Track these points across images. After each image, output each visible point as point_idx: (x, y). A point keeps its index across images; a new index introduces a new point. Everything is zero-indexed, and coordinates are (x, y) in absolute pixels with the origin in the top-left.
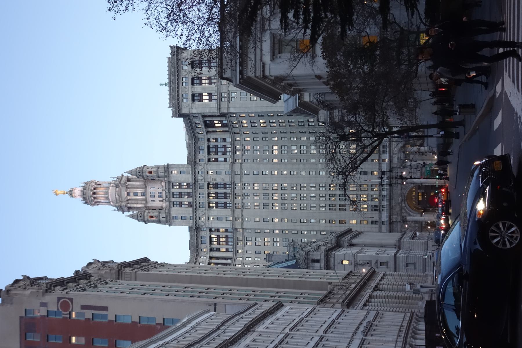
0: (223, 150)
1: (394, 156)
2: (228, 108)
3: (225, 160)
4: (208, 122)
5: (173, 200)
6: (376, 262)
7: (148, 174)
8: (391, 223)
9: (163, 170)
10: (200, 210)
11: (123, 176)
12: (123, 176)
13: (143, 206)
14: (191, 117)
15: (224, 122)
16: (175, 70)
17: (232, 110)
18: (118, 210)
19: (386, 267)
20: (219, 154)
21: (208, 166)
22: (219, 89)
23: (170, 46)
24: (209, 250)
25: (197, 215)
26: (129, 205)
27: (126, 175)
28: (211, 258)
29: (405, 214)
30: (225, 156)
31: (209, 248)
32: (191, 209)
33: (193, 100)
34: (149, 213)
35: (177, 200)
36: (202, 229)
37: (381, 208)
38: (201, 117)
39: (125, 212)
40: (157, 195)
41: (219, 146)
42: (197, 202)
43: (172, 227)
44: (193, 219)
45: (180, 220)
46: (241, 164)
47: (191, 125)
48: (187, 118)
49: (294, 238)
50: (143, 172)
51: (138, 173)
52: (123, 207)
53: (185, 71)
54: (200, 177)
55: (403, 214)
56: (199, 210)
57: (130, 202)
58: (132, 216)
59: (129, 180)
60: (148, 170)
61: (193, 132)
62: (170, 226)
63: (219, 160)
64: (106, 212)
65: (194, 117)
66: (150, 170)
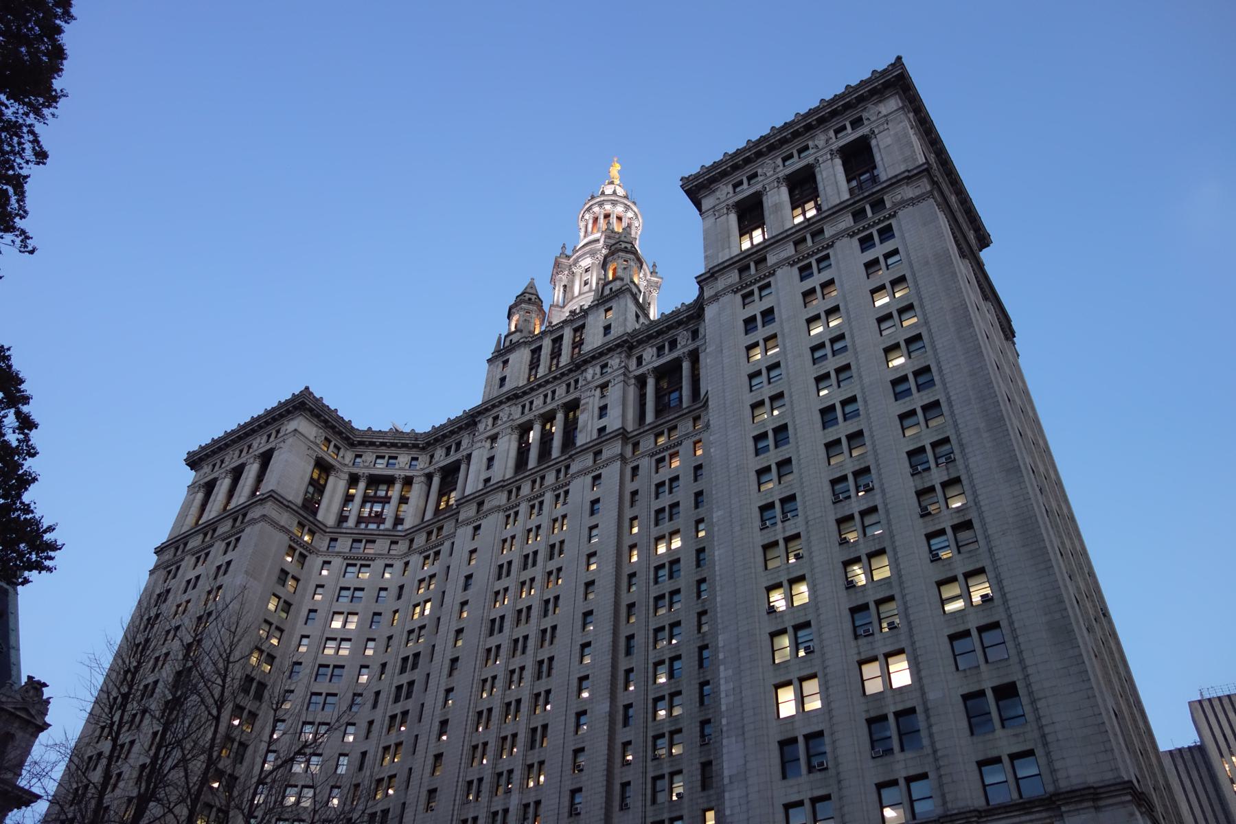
45: (499, 377)
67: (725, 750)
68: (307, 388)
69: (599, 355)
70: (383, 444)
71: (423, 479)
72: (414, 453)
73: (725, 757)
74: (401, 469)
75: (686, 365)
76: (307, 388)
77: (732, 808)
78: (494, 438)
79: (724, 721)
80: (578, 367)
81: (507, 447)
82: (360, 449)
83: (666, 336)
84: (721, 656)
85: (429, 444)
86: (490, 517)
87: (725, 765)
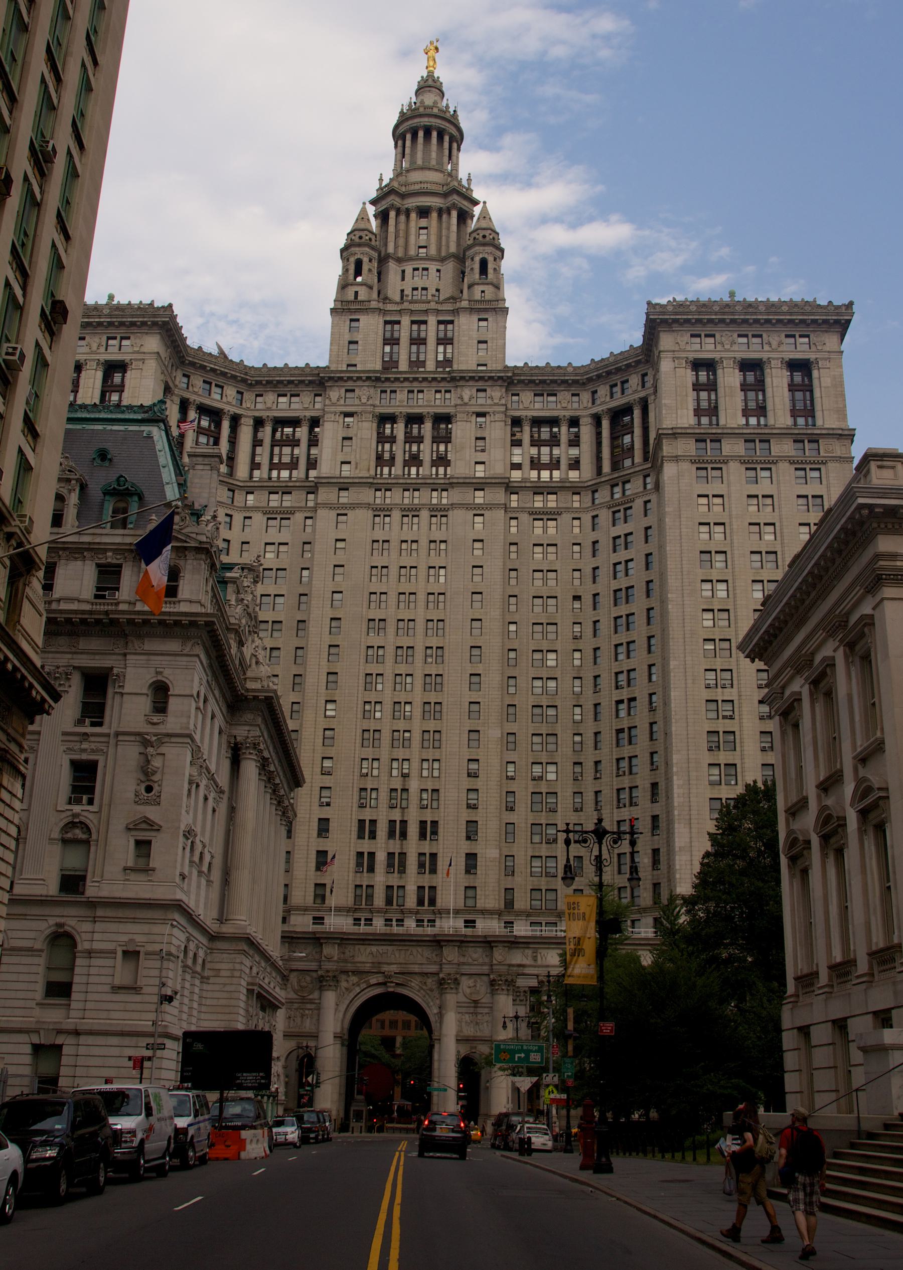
0: (545, 459)
1: (529, 952)
2: (676, 459)
3: (517, 467)
4: (627, 419)
5: (406, 321)
6: (151, 825)
7: (477, 259)
8: (317, 940)
9: (488, 296)
10: (375, 393)
11: (476, 203)
12: (476, 203)
13: (391, 249)
14: (642, 369)
15: (628, 463)
16: (784, 314)
17: (669, 471)
18: (381, 189)
19: (130, 863)
20: (534, 451)
21: (498, 417)
22: (733, 434)
23: (851, 303)
24: (257, 414)
25: (359, 383)
26: (392, 214)
27: (477, 210)
28: (235, 420)
29: (344, 984)
30: (527, 465)
31: (264, 414)
32: (379, 367)
33: (697, 365)
34: (370, 261)
35: (404, 331)
36: (318, 399)
37: (363, 916)
39: (373, 208)
40: (420, 283)
41: (556, 451)
42: (397, 384)
43: (327, 320)
44: (347, 371)
45: (347, 337)
46: (506, 508)
47: (618, 370)
48: (645, 356)
49: (282, 653)
50: (484, 245)
51: (482, 233)
52: (390, 202)
53: (780, 344)
54: (467, 393)
55: (343, 977)
56: (372, 390)
57: (402, 218)
58: (363, 217)
59: (464, 216)
60: (490, 259)
61: (599, 377)
62: (333, 311)
63: (517, 451)
64: (377, 161)
65: (646, 374)
66: (491, 266)
67: (676, 831)
68: (170, 306)
69: (482, 379)
70: (213, 370)
71: (251, 422)
72: (242, 387)
73: (676, 835)
74: (229, 403)
76: (170, 306)
77: (681, 865)
79: (676, 813)
84: (675, 769)
85: (259, 383)
86: (357, 511)
87: (676, 840)
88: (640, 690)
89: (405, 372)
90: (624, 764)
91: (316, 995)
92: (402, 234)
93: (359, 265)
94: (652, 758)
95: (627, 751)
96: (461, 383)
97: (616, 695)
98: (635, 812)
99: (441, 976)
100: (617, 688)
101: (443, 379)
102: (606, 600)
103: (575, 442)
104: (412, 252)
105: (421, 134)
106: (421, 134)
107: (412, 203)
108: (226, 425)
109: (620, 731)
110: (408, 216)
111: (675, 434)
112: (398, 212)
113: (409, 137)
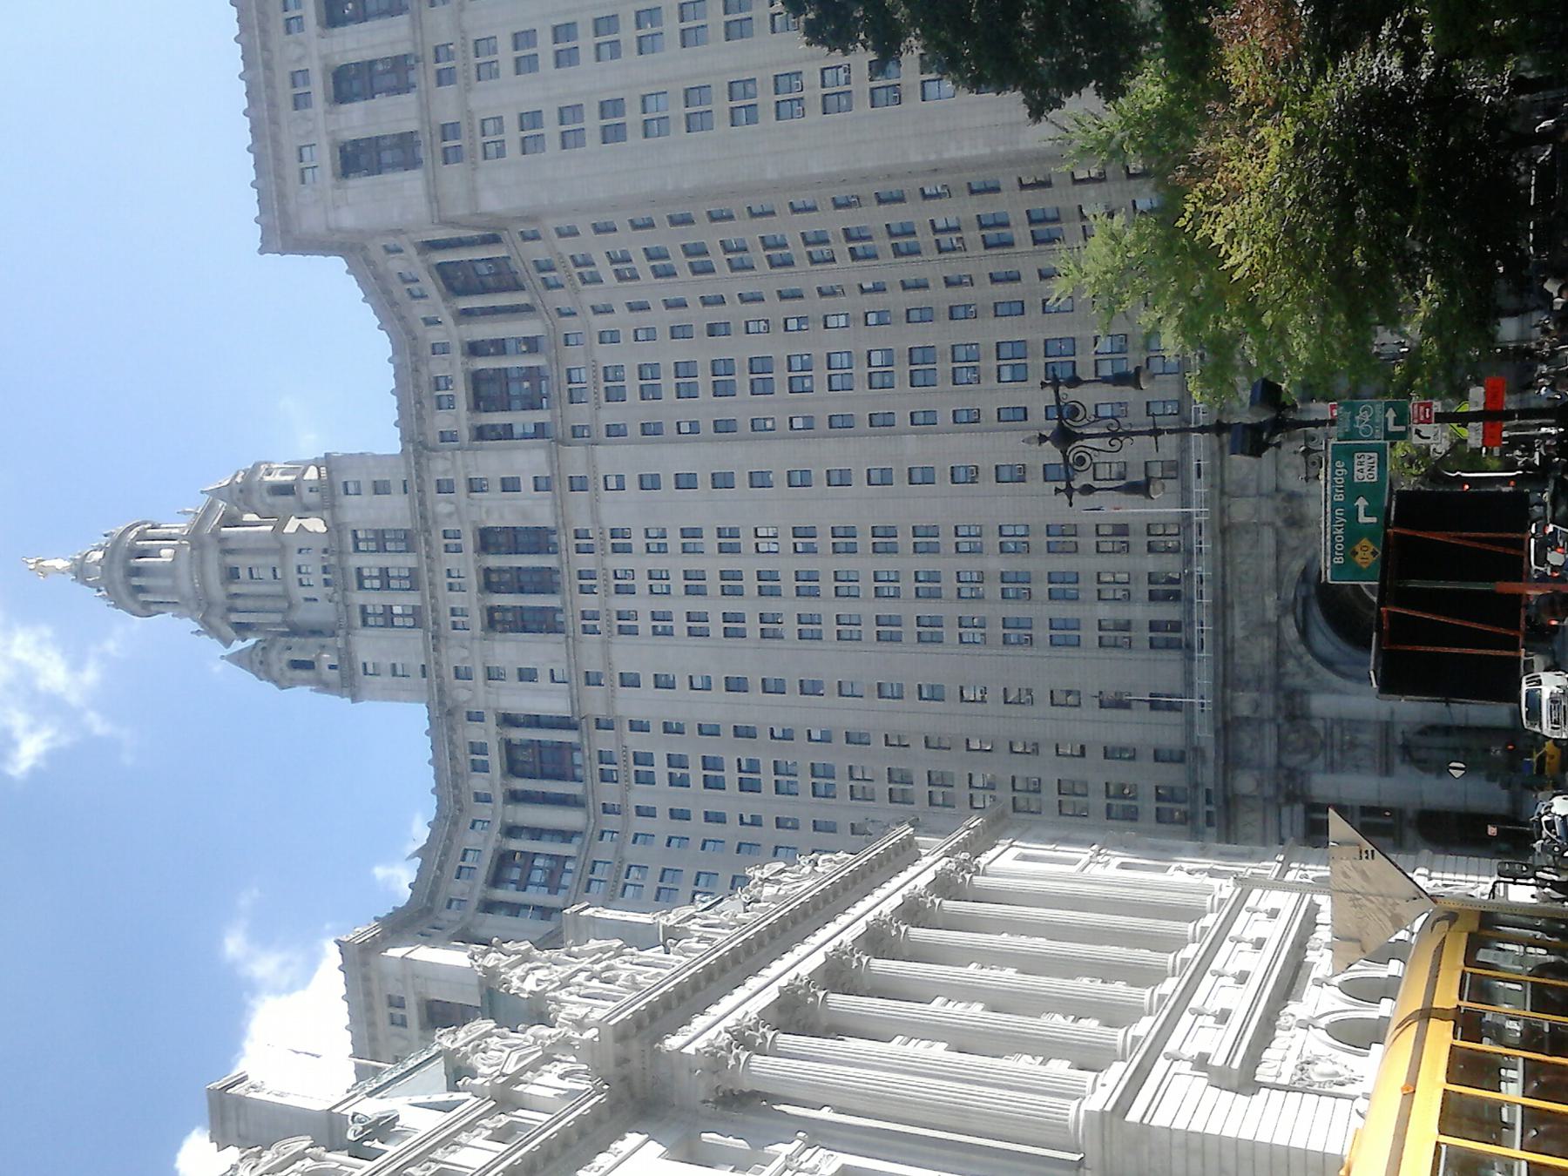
2: (473, 193)
7: (269, 500)
13: (278, 618)
14: (376, 252)
17: (491, 202)
20: (517, 403)
25: (443, 660)
29: (1299, 681)
32: (418, 633)
35: (376, 601)
38: (412, 252)
43: (365, 706)
45: (387, 679)
55: (1288, 681)
57: (239, 603)
58: (238, 659)
61: (402, 318)
62: (354, 699)
63: (518, 430)
70: (440, 867)
74: (486, 840)
75: (482, 364)
78: (492, 675)
80: (428, 531)
81: (510, 651)
82: (441, 900)
83: (426, 391)
88: (833, 222)
89: (423, 596)
90: (945, 239)
91: (1318, 725)
92: (258, 604)
93: (296, 665)
94: (932, 197)
95: (925, 238)
96: (429, 515)
97: (844, 260)
98: (1017, 217)
99: (1279, 523)
100: (833, 260)
101: (427, 542)
102: (709, 285)
103: (500, 347)
104: (278, 589)
105: (136, 581)
106: (136, 581)
107: (217, 591)
108: (514, 845)
109: (898, 252)
110: (236, 595)
111: (434, 198)
112: (232, 609)
113: (142, 597)
